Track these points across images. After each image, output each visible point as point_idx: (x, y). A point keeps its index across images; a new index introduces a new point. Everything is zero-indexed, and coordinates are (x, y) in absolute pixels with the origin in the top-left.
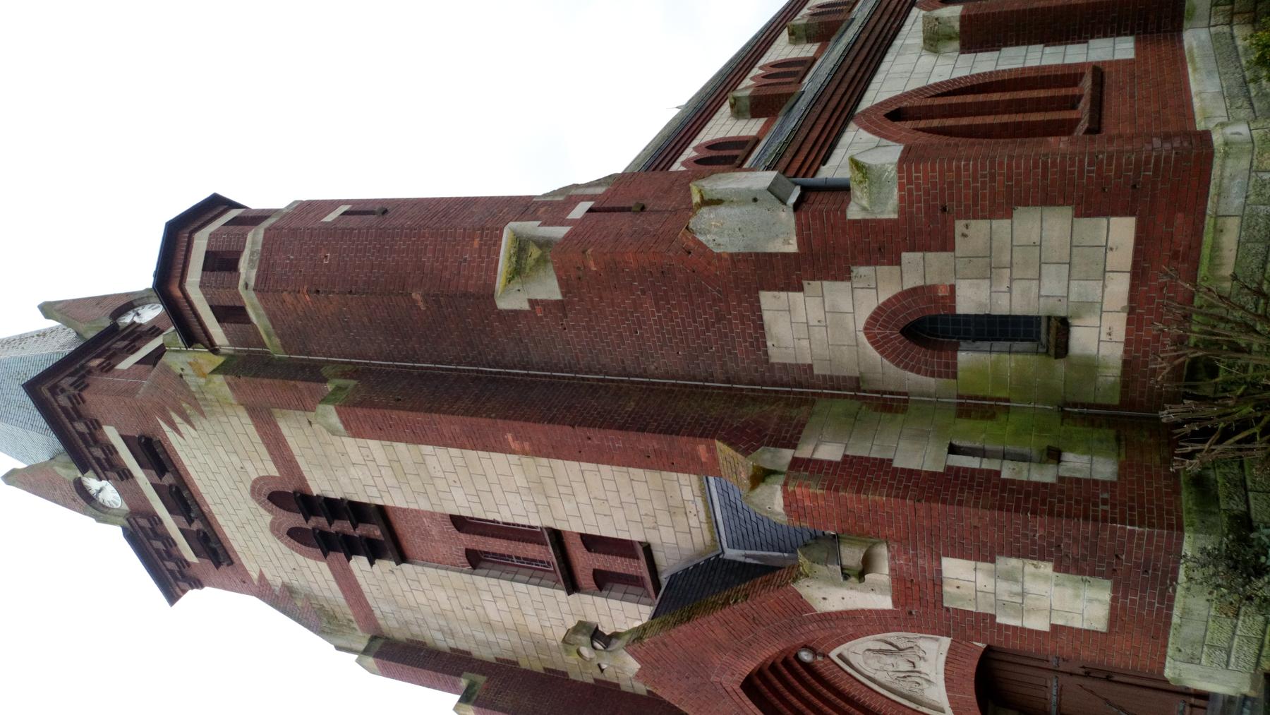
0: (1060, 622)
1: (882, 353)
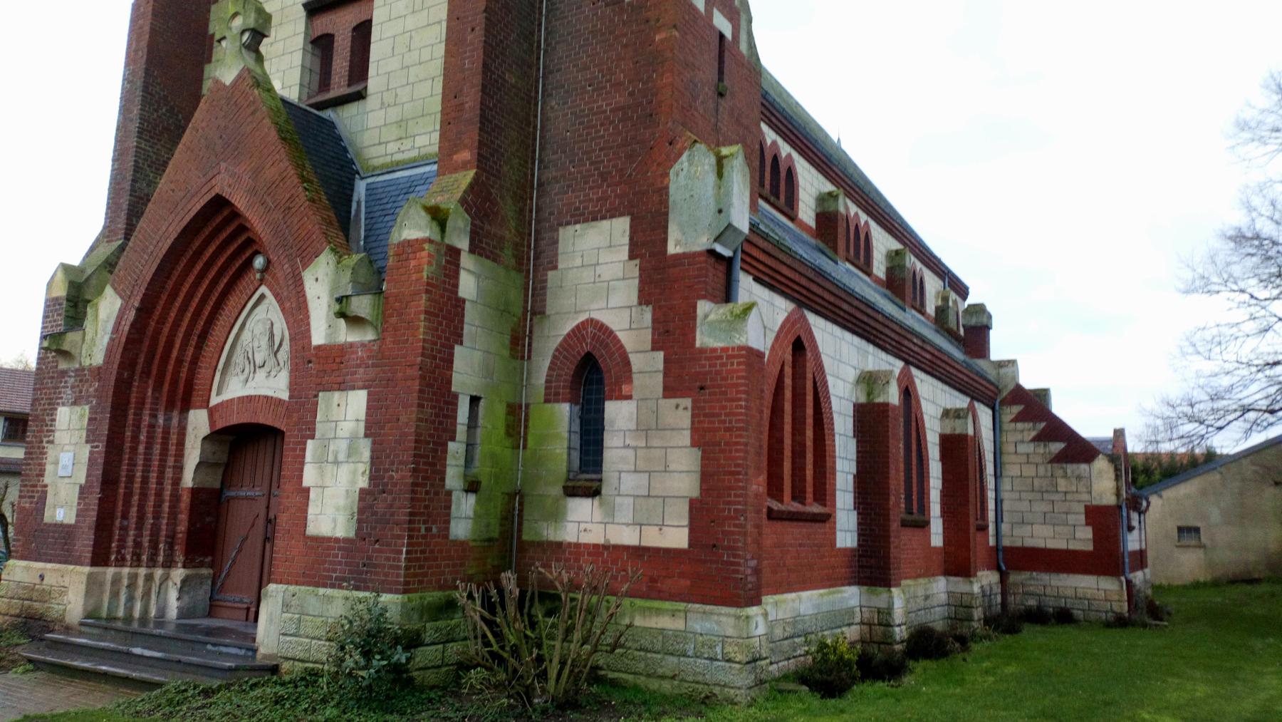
0: (312, 495)
1: (568, 335)
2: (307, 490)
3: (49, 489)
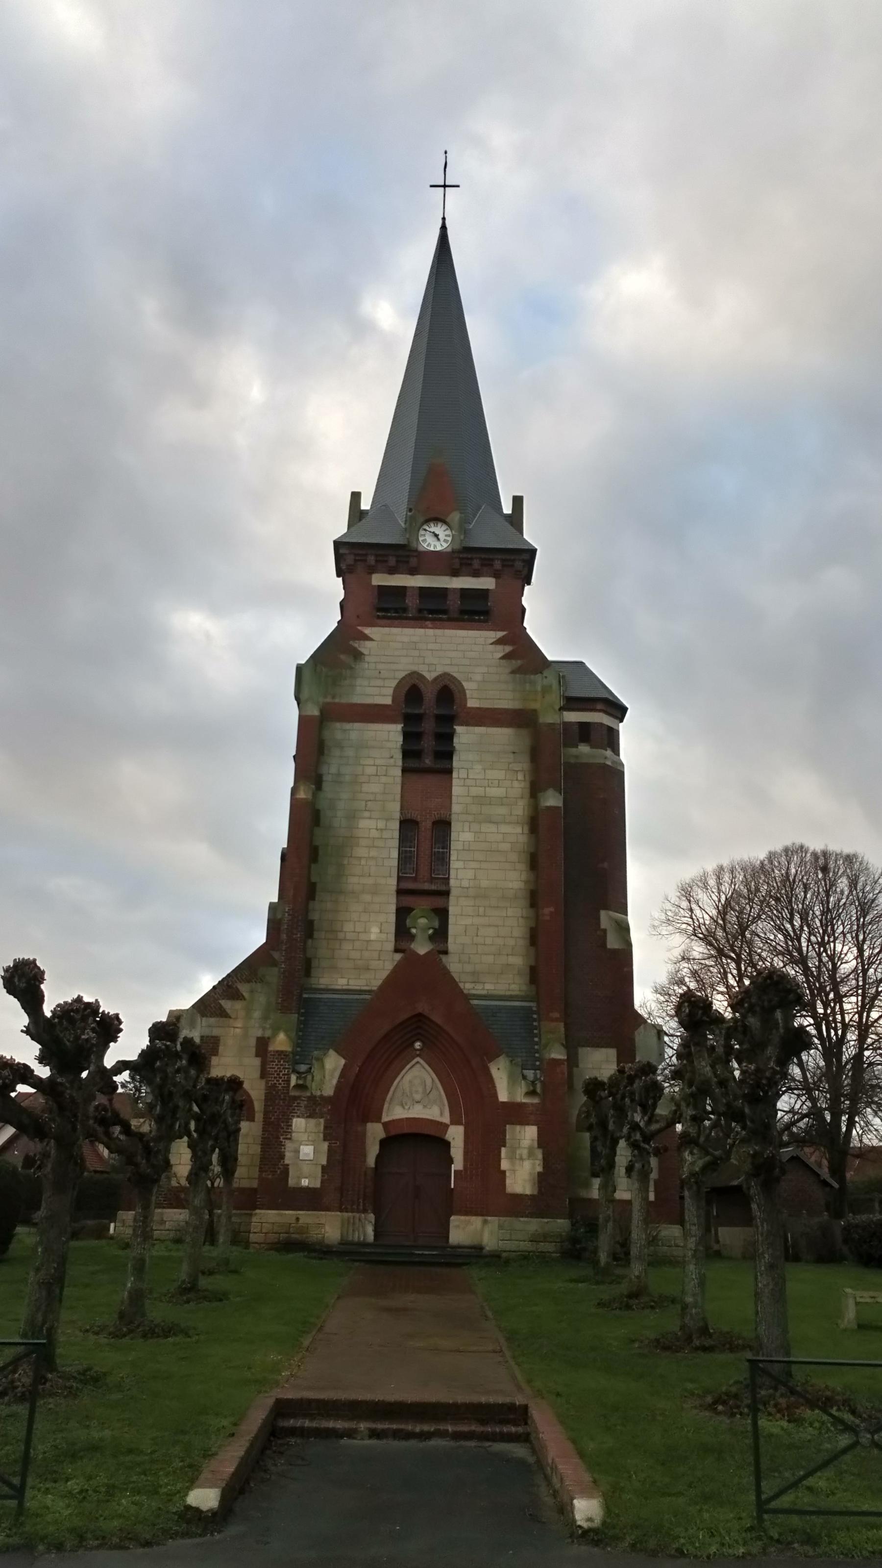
0: (508, 1174)
2: (504, 1172)
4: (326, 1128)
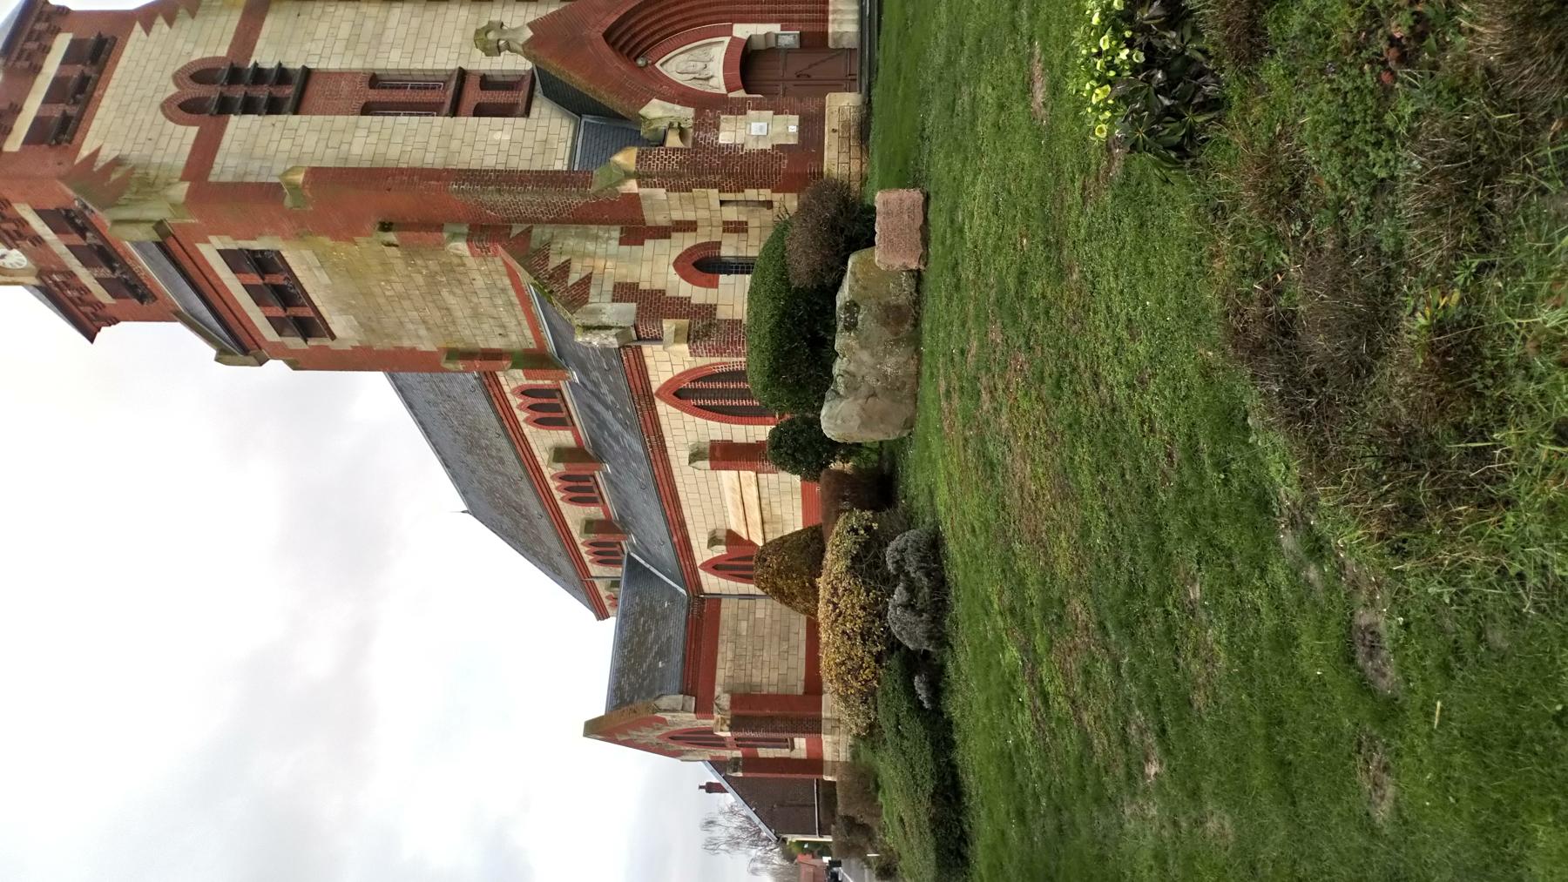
3: (775, 143)
4: (731, 113)
